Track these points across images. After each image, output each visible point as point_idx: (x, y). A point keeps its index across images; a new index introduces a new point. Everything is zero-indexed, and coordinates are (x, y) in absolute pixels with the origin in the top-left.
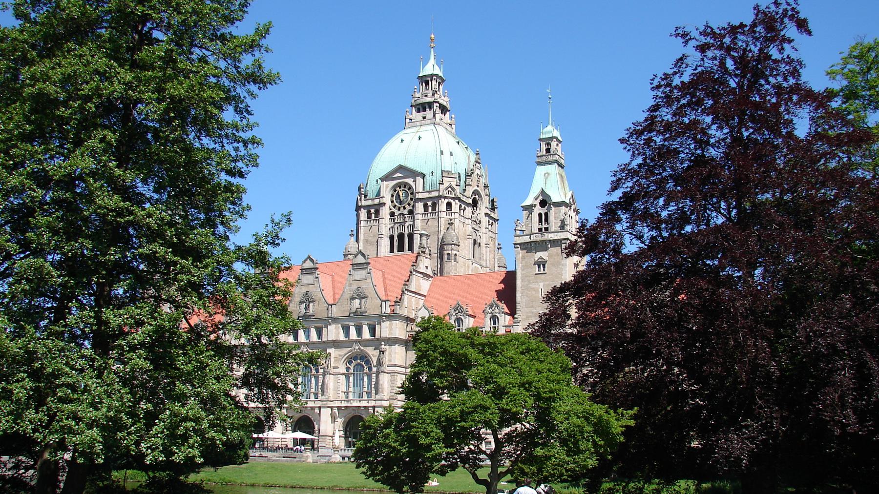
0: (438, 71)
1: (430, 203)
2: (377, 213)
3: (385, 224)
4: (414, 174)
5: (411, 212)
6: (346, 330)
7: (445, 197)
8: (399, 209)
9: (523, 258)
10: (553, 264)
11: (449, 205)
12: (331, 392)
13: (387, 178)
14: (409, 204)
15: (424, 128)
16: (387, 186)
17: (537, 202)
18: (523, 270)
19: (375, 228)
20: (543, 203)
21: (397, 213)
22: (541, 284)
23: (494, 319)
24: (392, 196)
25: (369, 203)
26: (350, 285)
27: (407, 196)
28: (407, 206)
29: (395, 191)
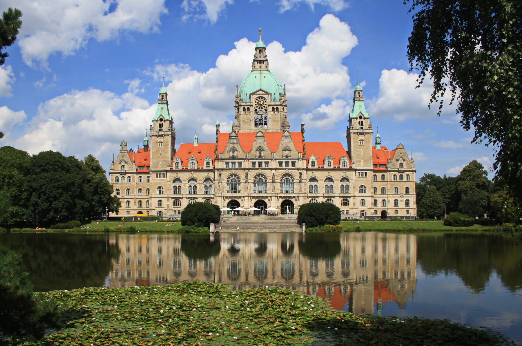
1: (275, 107)
2: (248, 109)
4: (267, 93)
5: (266, 110)
8: (259, 108)
9: (354, 138)
10: (366, 142)
11: (283, 108)
13: (254, 93)
15: (262, 72)
16: (253, 98)
17: (358, 117)
20: (360, 118)
21: (258, 110)
22: (362, 150)
23: (345, 162)
25: (244, 104)
26: (282, 145)
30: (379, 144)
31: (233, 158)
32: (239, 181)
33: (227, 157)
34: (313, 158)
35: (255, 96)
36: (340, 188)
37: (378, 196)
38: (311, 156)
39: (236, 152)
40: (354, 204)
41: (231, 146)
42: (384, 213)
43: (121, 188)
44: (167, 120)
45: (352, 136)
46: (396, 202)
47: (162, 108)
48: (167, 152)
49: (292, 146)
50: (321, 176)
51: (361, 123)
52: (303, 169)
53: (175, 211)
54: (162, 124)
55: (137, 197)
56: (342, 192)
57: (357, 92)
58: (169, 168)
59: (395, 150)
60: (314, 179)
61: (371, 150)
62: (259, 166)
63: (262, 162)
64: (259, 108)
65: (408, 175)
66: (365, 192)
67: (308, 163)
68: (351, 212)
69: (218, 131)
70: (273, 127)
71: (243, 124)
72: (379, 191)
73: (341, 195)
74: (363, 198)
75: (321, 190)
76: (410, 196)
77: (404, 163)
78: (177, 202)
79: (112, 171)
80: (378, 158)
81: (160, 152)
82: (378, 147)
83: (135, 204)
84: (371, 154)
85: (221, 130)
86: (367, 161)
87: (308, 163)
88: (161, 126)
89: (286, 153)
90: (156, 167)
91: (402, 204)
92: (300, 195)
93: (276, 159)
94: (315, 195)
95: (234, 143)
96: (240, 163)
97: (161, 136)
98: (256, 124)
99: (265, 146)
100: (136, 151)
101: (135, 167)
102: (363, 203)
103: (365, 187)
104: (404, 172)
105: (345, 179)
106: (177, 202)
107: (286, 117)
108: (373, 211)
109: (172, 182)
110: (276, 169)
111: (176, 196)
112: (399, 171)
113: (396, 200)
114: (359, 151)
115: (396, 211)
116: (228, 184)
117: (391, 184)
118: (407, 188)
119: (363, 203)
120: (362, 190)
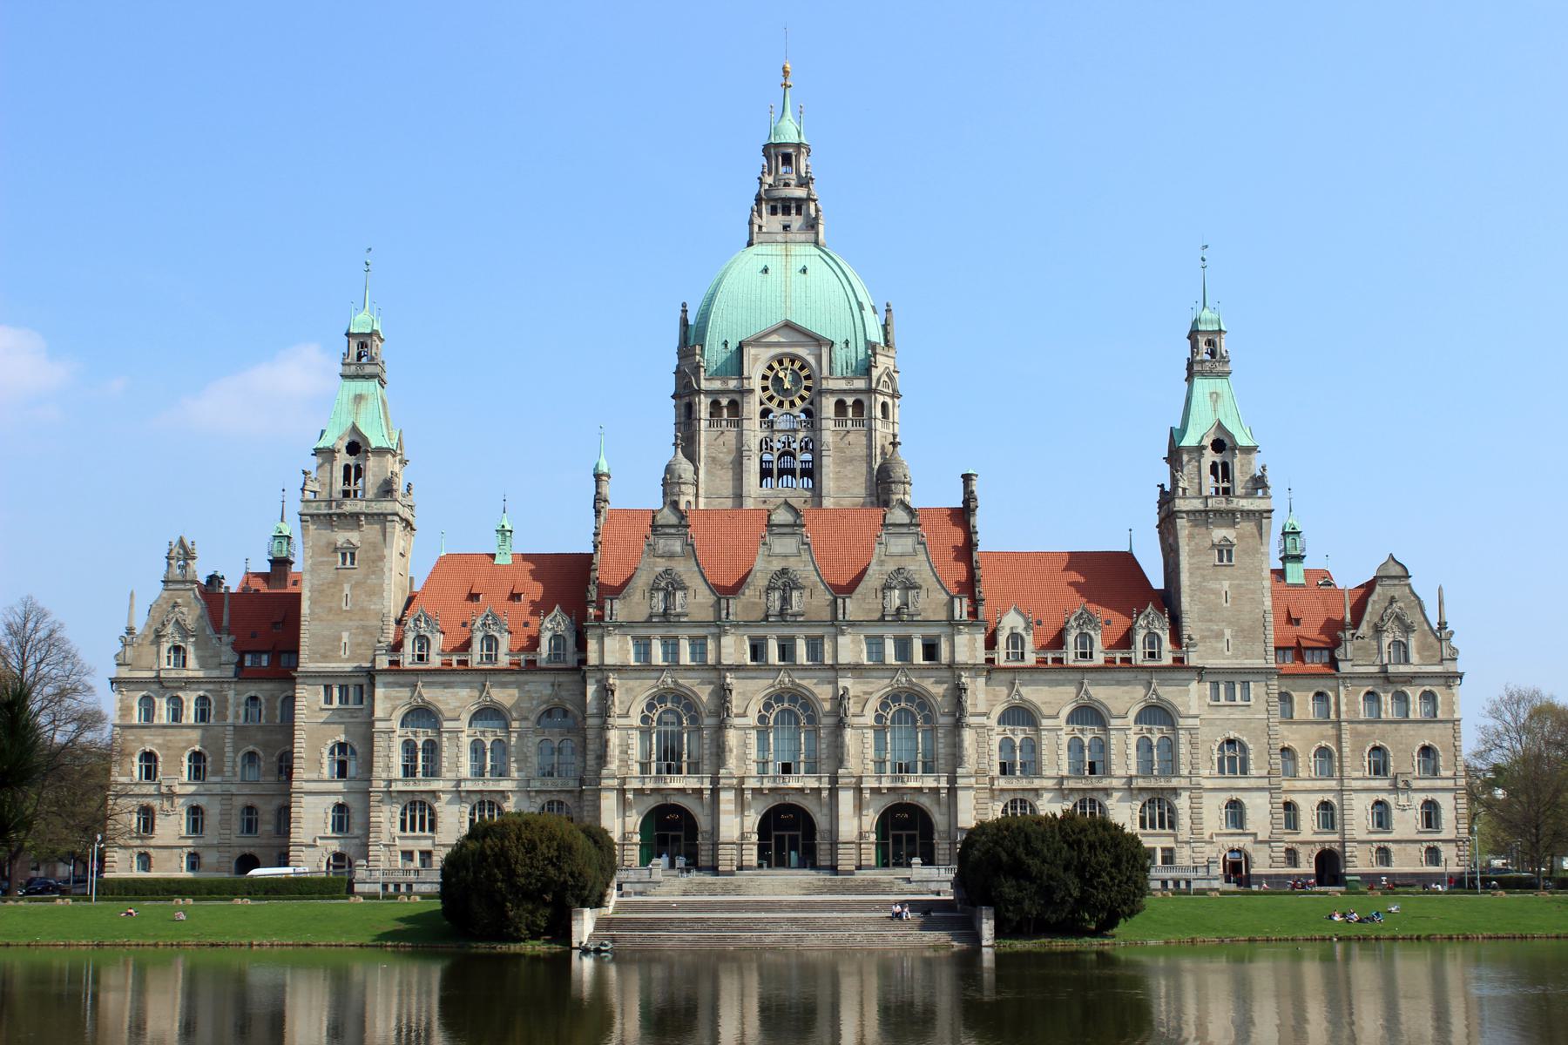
0: (803, 140)
1: (850, 401)
2: (735, 407)
3: (754, 431)
4: (817, 341)
6: (876, 644)
7: (881, 393)
8: (781, 404)
10: (1245, 552)
11: (884, 405)
12: (852, 765)
13: (757, 342)
14: (802, 398)
15: (795, 249)
18: (1192, 554)
19: (731, 435)
20: (1218, 446)
21: (777, 411)
22: (1226, 584)
23: (1153, 639)
24: (765, 377)
25: (717, 385)
26: (881, 563)
27: (796, 380)
28: (798, 401)
29: (771, 368)
30: (1299, 558)
31: (667, 617)
32: (694, 720)
33: (641, 615)
34: (1012, 621)
35: (766, 354)
36: (1133, 751)
37: (1299, 785)
38: (1004, 612)
39: (679, 594)
40: (1196, 819)
41: (661, 565)
42: (1329, 866)
43: (165, 747)
44: (381, 452)
45: (1183, 524)
46: (1382, 814)
47: (359, 398)
48: (377, 592)
49: (919, 568)
50: (1053, 700)
51: (1222, 471)
52: (974, 669)
53: (408, 855)
54: (358, 468)
55: (234, 789)
56: (1146, 769)
57: (1202, 340)
58: (383, 662)
59: (1369, 587)
60: (1021, 714)
61: (1267, 583)
62: (783, 657)
63: (793, 639)
64: (781, 404)
65: (1429, 697)
66: (1244, 771)
67: (991, 643)
68: (1184, 856)
69: (599, 500)
70: (842, 484)
71: (708, 472)
72: (1307, 763)
73: (1141, 783)
74: (1235, 796)
75: (1056, 759)
76: (1439, 783)
77: (1413, 643)
78: (420, 812)
79: (125, 673)
80: (1298, 621)
81: (347, 589)
82: (1295, 574)
83: (224, 821)
84: (1268, 603)
85: (618, 498)
86: (1245, 634)
87: (991, 643)
88: (353, 473)
89: (895, 598)
90: (325, 658)
91: (1407, 821)
92: (961, 782)
93: (852, 624)
94: (1024, 784)
95: (671, 556)
96: (698, 645)
97: (355, 516)
98: (765, 473)
99: (804, 569)
100: (233, 583)
101: (228, 655)
102: (1236, 811)
103: (1244, 748)
104: (1411, 679)
105: (1158, 713)
106: (420, 812)
107: (894, 444)
108: (1279, 851)
109: (396, 724)
110: (856, 669)
111: (411, 788)
112: (1386, 678)
113: (1378, 803)
114: (1213, 591)
115: (1384, 855)
116: (645, 733)
117: (1356, 734)
118: (1427, 751)
119: (1236, 811)
120: (1232, 760)
